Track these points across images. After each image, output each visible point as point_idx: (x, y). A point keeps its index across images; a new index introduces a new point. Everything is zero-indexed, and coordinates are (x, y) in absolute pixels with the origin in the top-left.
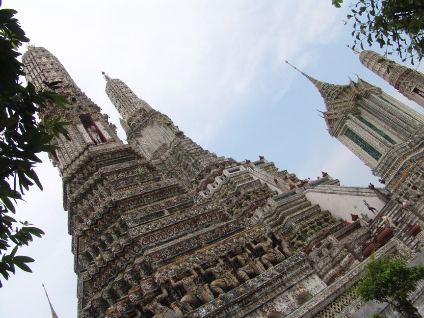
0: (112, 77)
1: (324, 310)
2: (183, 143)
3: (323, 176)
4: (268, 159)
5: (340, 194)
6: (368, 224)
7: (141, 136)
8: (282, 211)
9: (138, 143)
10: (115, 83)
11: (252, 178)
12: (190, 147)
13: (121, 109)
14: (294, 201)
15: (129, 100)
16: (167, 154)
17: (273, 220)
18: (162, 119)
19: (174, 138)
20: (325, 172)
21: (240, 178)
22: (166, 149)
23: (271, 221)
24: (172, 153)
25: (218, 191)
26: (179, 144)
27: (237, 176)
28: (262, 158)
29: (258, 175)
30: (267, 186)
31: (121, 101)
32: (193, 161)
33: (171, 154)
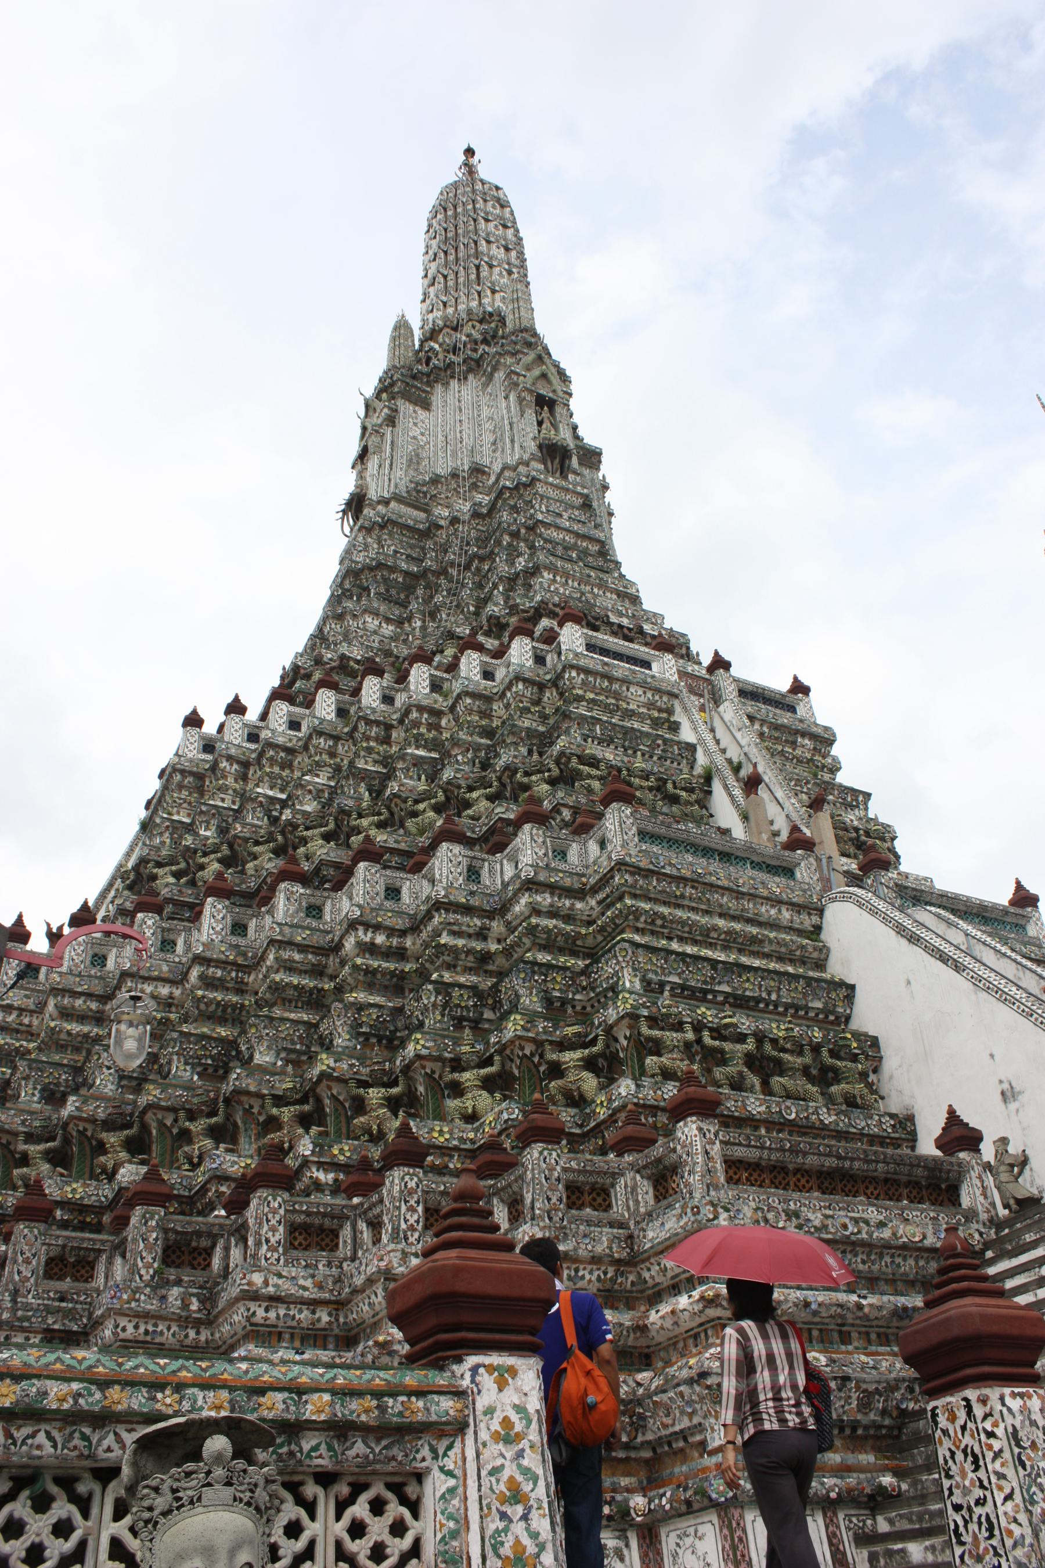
0: (484, 172)
1: (378, 1489)
2: (540, 488)
3: (1012, 903)
4: (822, 709)
5: (976, 981)
6: (1003, 1213)
7: (426, 406)
8: (635, 896)
9: (391, 421)
10: (474, 191)
11: (675, 727)
12: (560, 515)
13: (431, 289)
14: (739, 895)
15: (478, 267)
16: (464, 508)
17: (568, 918)
18: (537, 372)
19: (526, 457)
20: (1032, 888)
21: (617, 696)
22: (474, 486)
23: (553, 914)
24: (484, 511)
25: (488, 699)
26: (526, 486)
27: (611, 679)
28: (799, 688)
29: (719, 736)
30: (710, 793)
31: (451, 258)
32: (521, 563)
33: (476, 515)
